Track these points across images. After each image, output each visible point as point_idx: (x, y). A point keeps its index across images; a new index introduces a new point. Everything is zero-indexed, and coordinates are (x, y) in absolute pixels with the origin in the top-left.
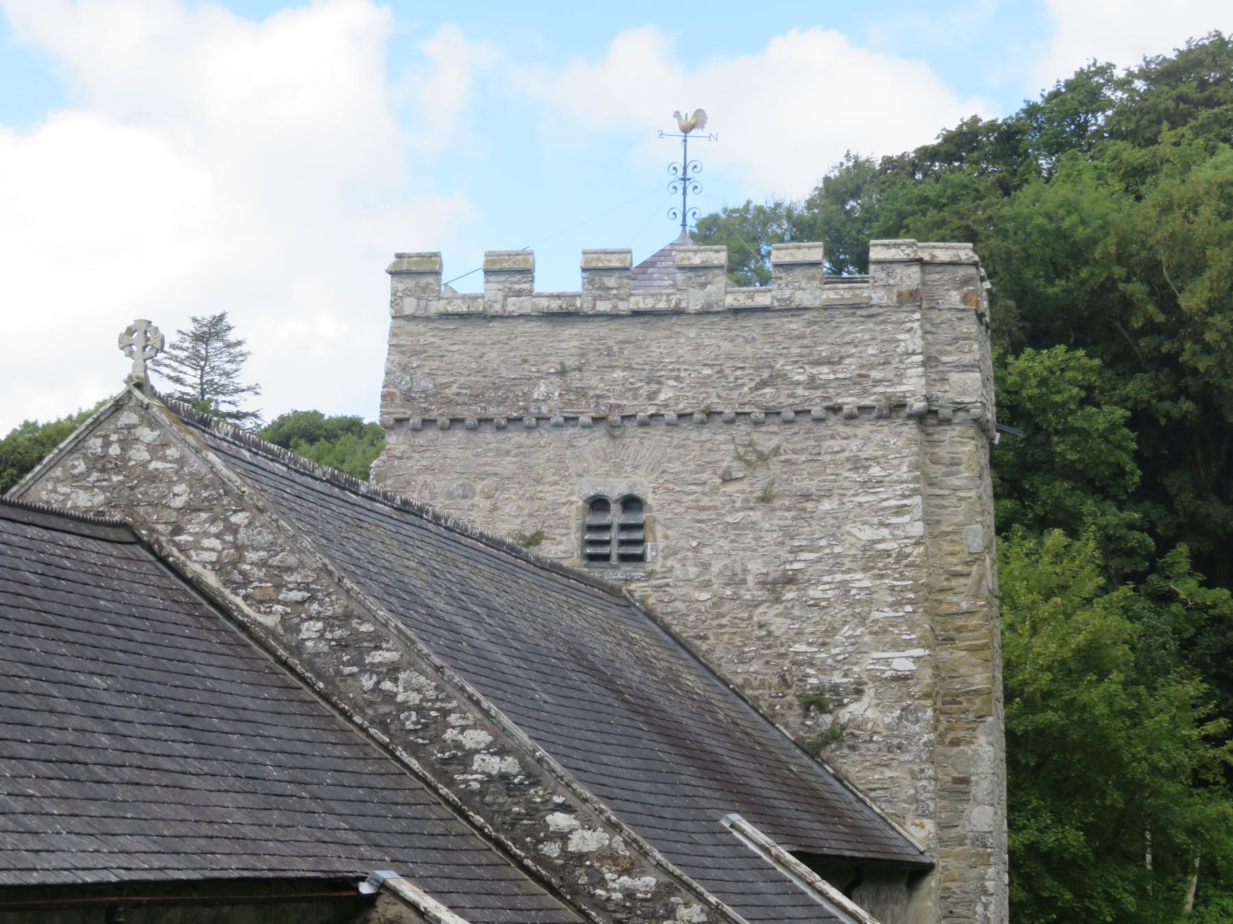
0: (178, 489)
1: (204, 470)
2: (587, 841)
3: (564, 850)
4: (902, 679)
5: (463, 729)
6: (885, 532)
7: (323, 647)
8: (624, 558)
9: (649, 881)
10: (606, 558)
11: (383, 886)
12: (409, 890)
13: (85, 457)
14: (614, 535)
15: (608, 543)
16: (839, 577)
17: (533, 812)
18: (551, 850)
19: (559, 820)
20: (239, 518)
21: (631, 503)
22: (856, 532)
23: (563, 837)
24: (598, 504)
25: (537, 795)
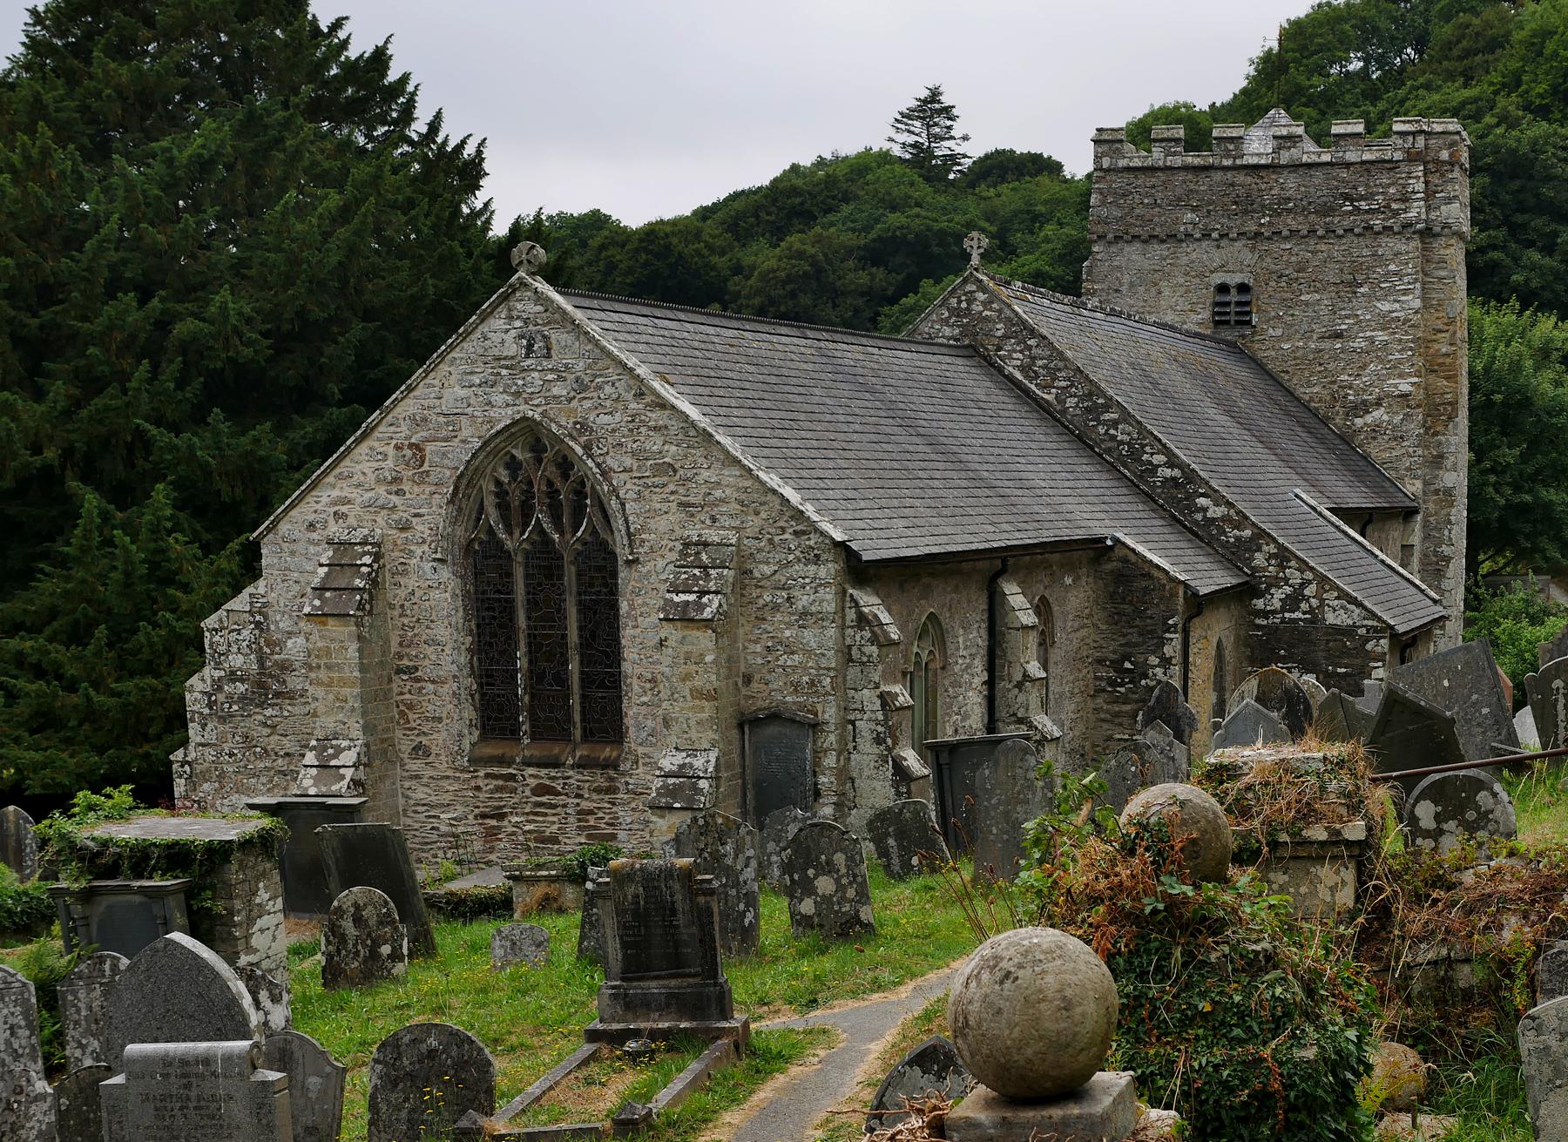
0: (998, 326)
1: (1012, 316)
2: (1216, 512)
3: (1205, 516)
4: (1404, 396)
5: (1152, 454)
6: (1397, 306)
7: (1078, 412)
8: (1238, 323)
9: (1248, 533)
10: (1227, 322)
11: (1117, 541)
12: (1129, 541)
13: (948, 309)
14: (1233, 309)
15: (1228, 313)
16: (1368, 334)
17: (1191, 497)
18: (1199, 517)
19: (1202, 501)
20: (1032, 342)
21: (1243, 288)
22: (1379, 305)
23: (1205, 510)
24: (1223, 289)
25: (1190, 488)
